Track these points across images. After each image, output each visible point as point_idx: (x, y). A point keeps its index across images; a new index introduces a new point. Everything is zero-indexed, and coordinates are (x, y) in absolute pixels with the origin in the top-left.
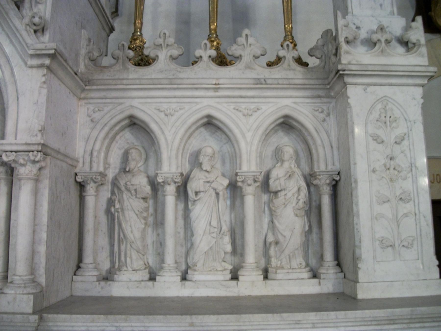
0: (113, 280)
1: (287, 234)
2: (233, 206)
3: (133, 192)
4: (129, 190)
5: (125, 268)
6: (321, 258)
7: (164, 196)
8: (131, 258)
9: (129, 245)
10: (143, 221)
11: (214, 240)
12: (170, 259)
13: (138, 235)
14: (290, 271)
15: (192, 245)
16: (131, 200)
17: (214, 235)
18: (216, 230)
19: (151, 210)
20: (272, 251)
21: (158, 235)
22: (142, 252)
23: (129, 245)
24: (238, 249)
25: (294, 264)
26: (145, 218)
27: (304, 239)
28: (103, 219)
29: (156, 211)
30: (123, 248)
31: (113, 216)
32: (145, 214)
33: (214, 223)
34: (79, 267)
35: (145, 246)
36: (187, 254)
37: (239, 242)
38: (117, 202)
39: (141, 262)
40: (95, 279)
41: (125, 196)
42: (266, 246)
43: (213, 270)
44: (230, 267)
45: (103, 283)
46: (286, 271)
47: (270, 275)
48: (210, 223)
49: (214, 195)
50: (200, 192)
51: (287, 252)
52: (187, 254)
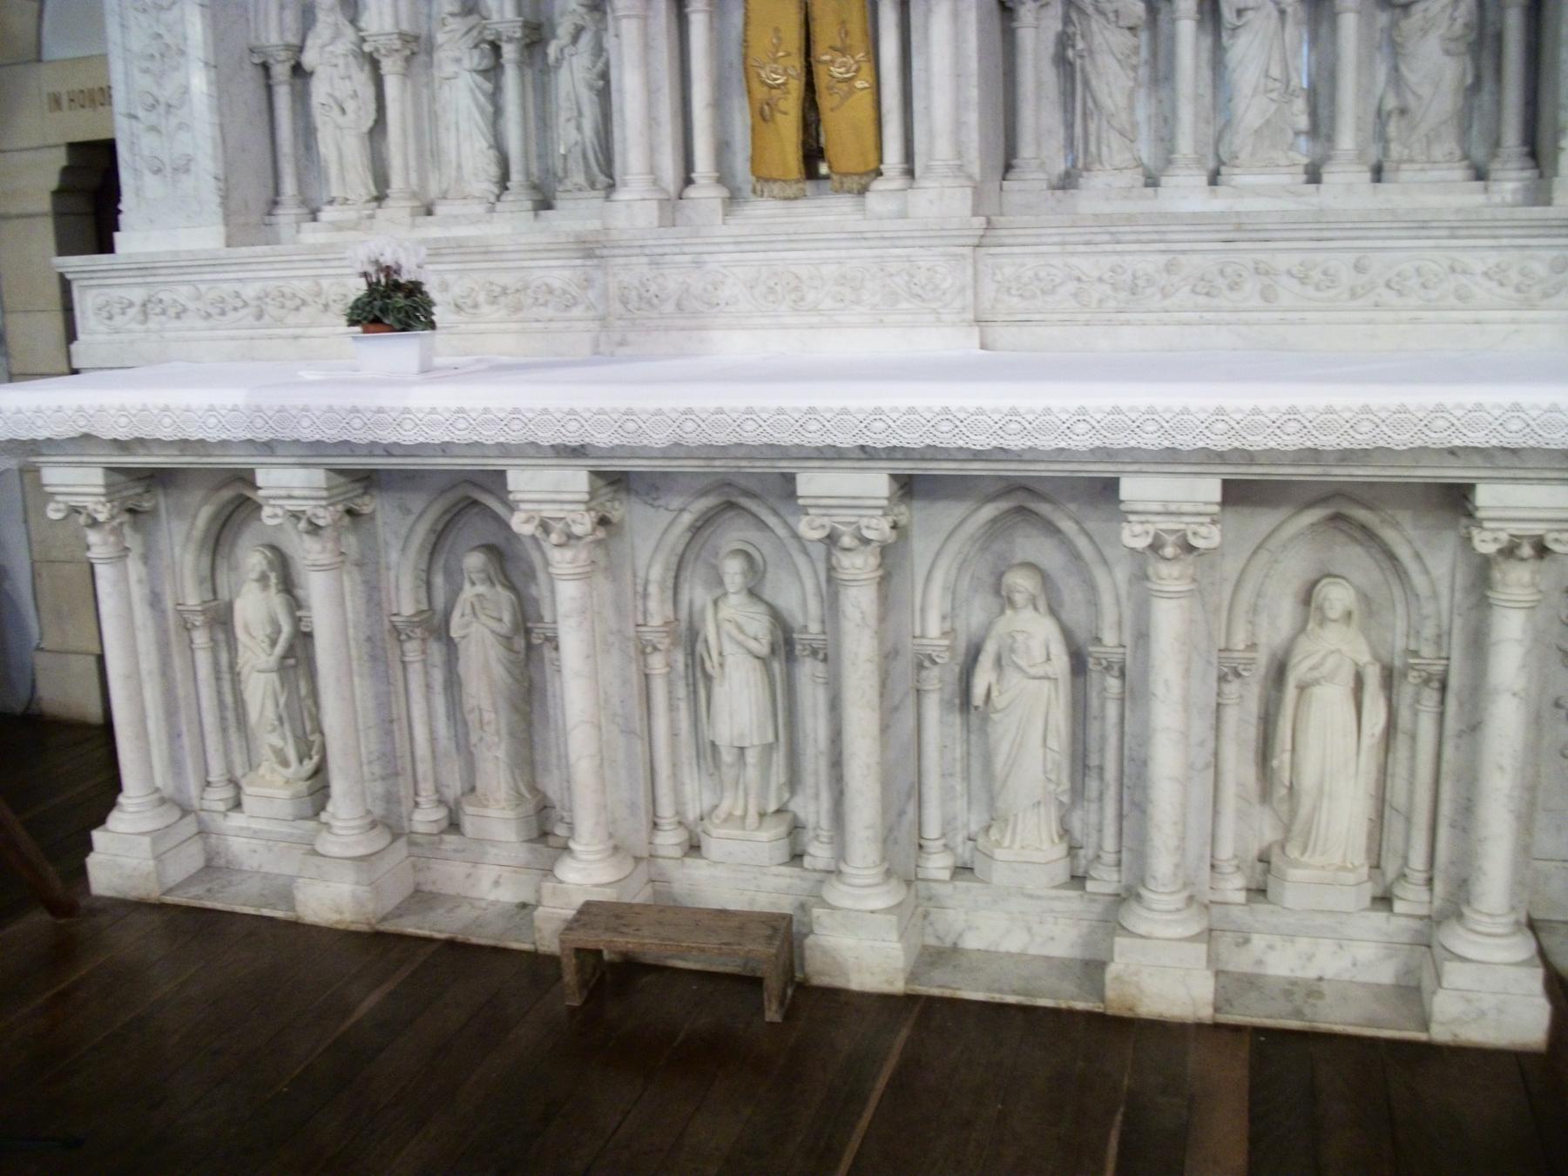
0: (1075, 187)
1: (1425, 91)
2: (1314, 40)
3: (1111, 16)
4: (1102, 13)
5: (1097, 166)
6: (1497, 143)
7: (1173, 21)
8: (1109, 146)
9: (1104, 123)
10: (1132, 74)
11: (1274, 106)
12: (1185, 145)
13: (1121, 100)
14: (1427, 166)
15: (1228, 124)
16: (1107, 33)
17: (1274, 95)
18: (1278, 85)
19: (1144, 53)
20: (1392, 129)
21: (1160, 101)
22: (1129, 136)
23: (1104, 123)
24: (1320, 127)
25: (1438, 152)
26: (1134, 68)
27: (1460, 103)
28: (1050, 75)
29: (1154, 54)
30: (1092, 127)
31: (1072, 64)
32: (1134, 61)
33: (1275, 71)
34: (1008, 167)
35: (1134, 125)
36: (1218, 140)
37: (1323, 112)
38: (1078, 37)
39: (1128, 155)
40: (1044, 185)
41: (1095, 27)
42: (1381, 116)
43: (1271, 166)
44: (1305, 161)
45: (1059, 193)
46: (1418, 166)
47: (1385, 175)
48: (1267, 70)
49: (1275, 14)
50: (1246, 9)
51: (1423, 128)
52: (1218, 140)
